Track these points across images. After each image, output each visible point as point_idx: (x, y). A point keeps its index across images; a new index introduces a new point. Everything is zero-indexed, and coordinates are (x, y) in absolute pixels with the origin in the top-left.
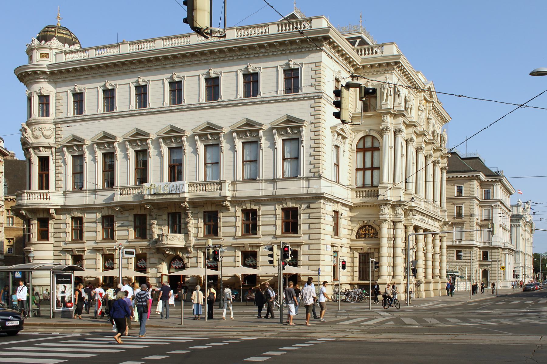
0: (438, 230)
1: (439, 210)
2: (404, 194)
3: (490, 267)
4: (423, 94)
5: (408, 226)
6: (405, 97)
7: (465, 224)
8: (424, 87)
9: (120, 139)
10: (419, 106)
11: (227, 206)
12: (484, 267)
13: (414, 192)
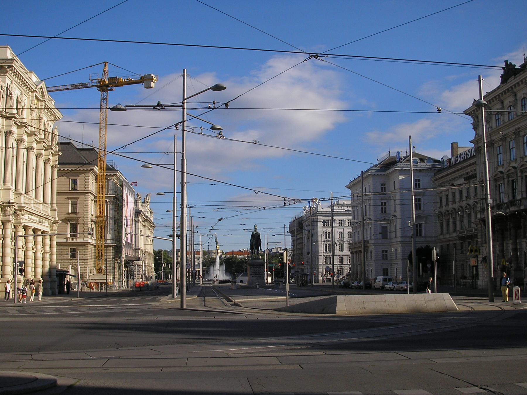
0: (48, 229)
1: (49, 209)
2: (14, 194)
4: (35, 94)
5: (17, 226)
6: (17, 98)
8: (36, 88)
10: (31, 106)
13: (24, 192)
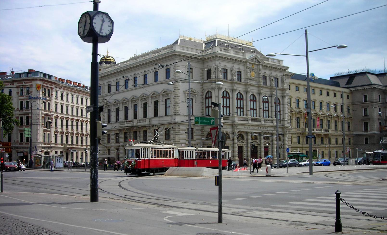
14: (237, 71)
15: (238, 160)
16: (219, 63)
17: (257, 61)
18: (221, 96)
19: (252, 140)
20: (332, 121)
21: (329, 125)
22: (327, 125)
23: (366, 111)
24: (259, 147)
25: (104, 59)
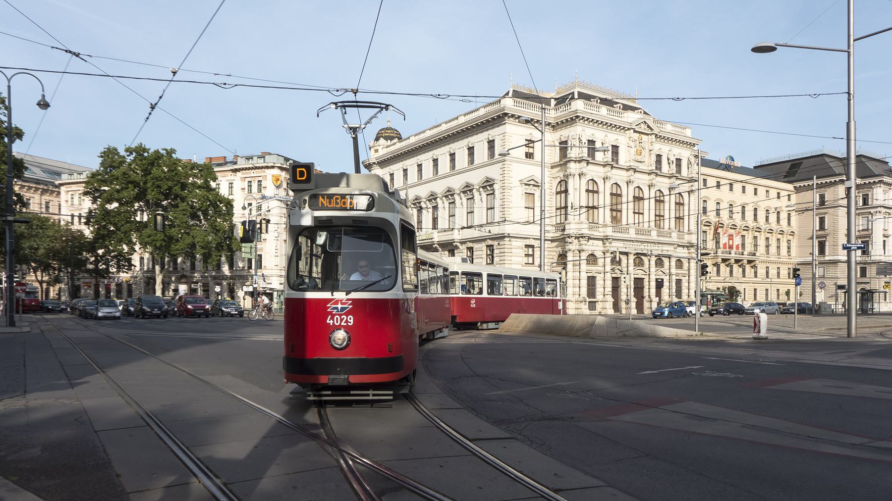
3: (869, 285)
7: (828, 237)
9: (457, 192)
11: (456, 246)
12: (861, 285)
14: (612, 145)
15: (611, 301)
16: (581, 129)
17: (648, 127)
18: (584, 188)
19: (635, 267)
20: (760, 238)
21: (756, 246)
22: (753, 246)
23: (822, 221)
24: (647, 280)
25: (382, 133)
